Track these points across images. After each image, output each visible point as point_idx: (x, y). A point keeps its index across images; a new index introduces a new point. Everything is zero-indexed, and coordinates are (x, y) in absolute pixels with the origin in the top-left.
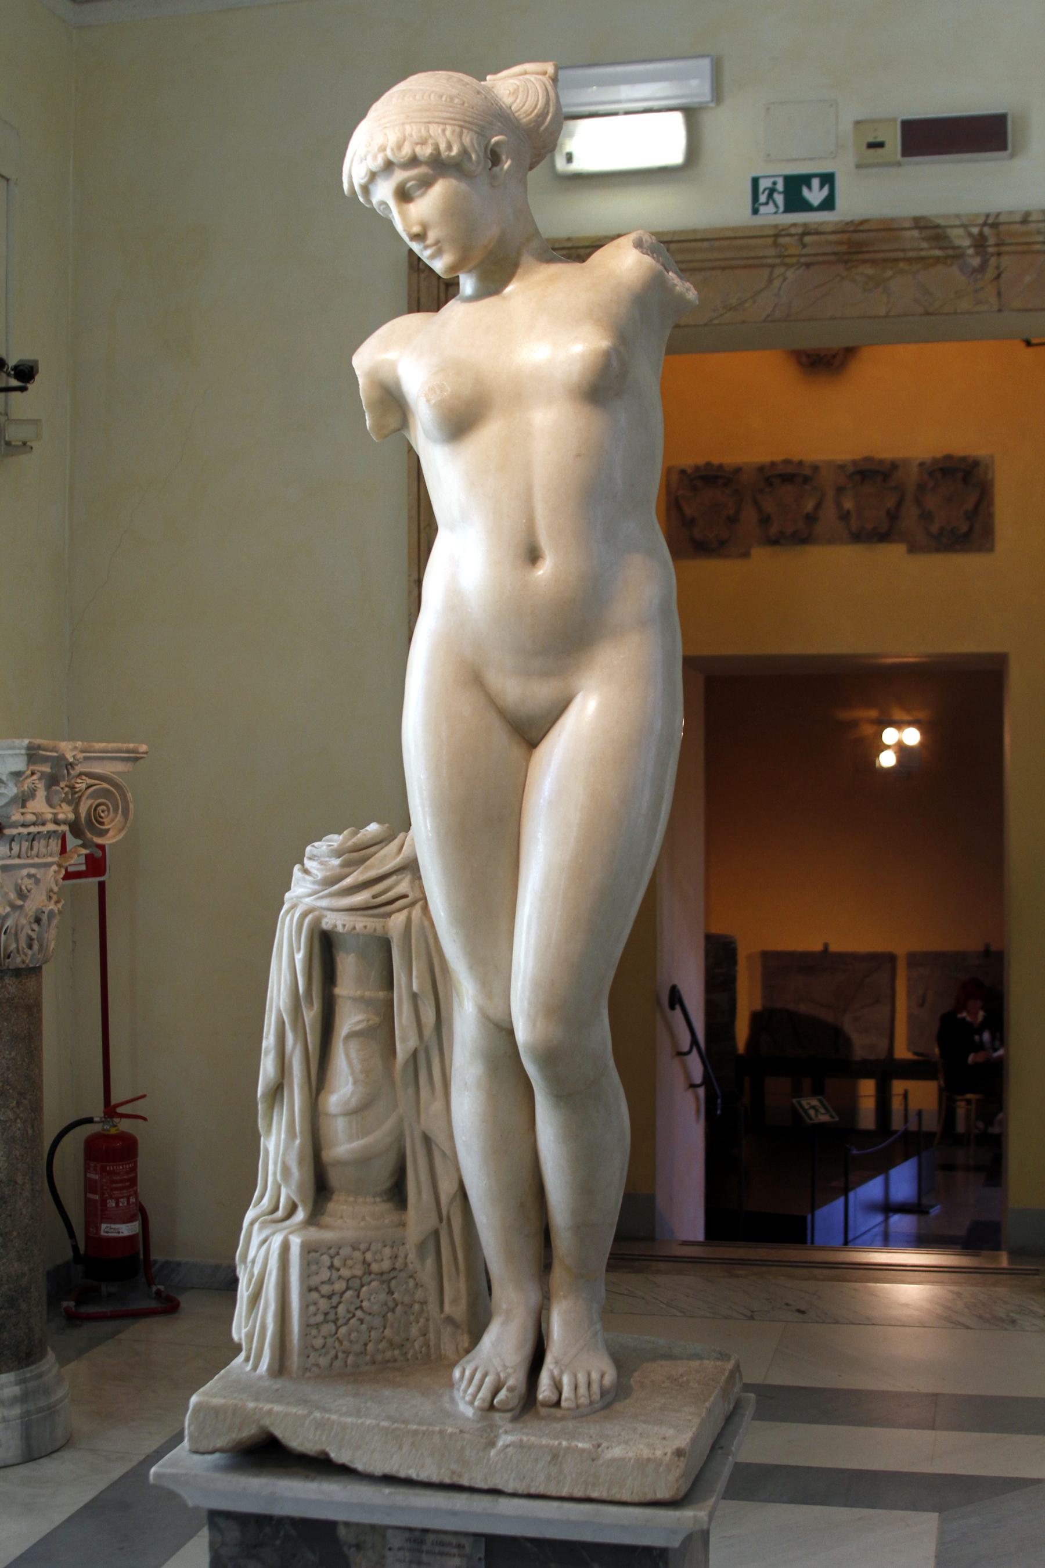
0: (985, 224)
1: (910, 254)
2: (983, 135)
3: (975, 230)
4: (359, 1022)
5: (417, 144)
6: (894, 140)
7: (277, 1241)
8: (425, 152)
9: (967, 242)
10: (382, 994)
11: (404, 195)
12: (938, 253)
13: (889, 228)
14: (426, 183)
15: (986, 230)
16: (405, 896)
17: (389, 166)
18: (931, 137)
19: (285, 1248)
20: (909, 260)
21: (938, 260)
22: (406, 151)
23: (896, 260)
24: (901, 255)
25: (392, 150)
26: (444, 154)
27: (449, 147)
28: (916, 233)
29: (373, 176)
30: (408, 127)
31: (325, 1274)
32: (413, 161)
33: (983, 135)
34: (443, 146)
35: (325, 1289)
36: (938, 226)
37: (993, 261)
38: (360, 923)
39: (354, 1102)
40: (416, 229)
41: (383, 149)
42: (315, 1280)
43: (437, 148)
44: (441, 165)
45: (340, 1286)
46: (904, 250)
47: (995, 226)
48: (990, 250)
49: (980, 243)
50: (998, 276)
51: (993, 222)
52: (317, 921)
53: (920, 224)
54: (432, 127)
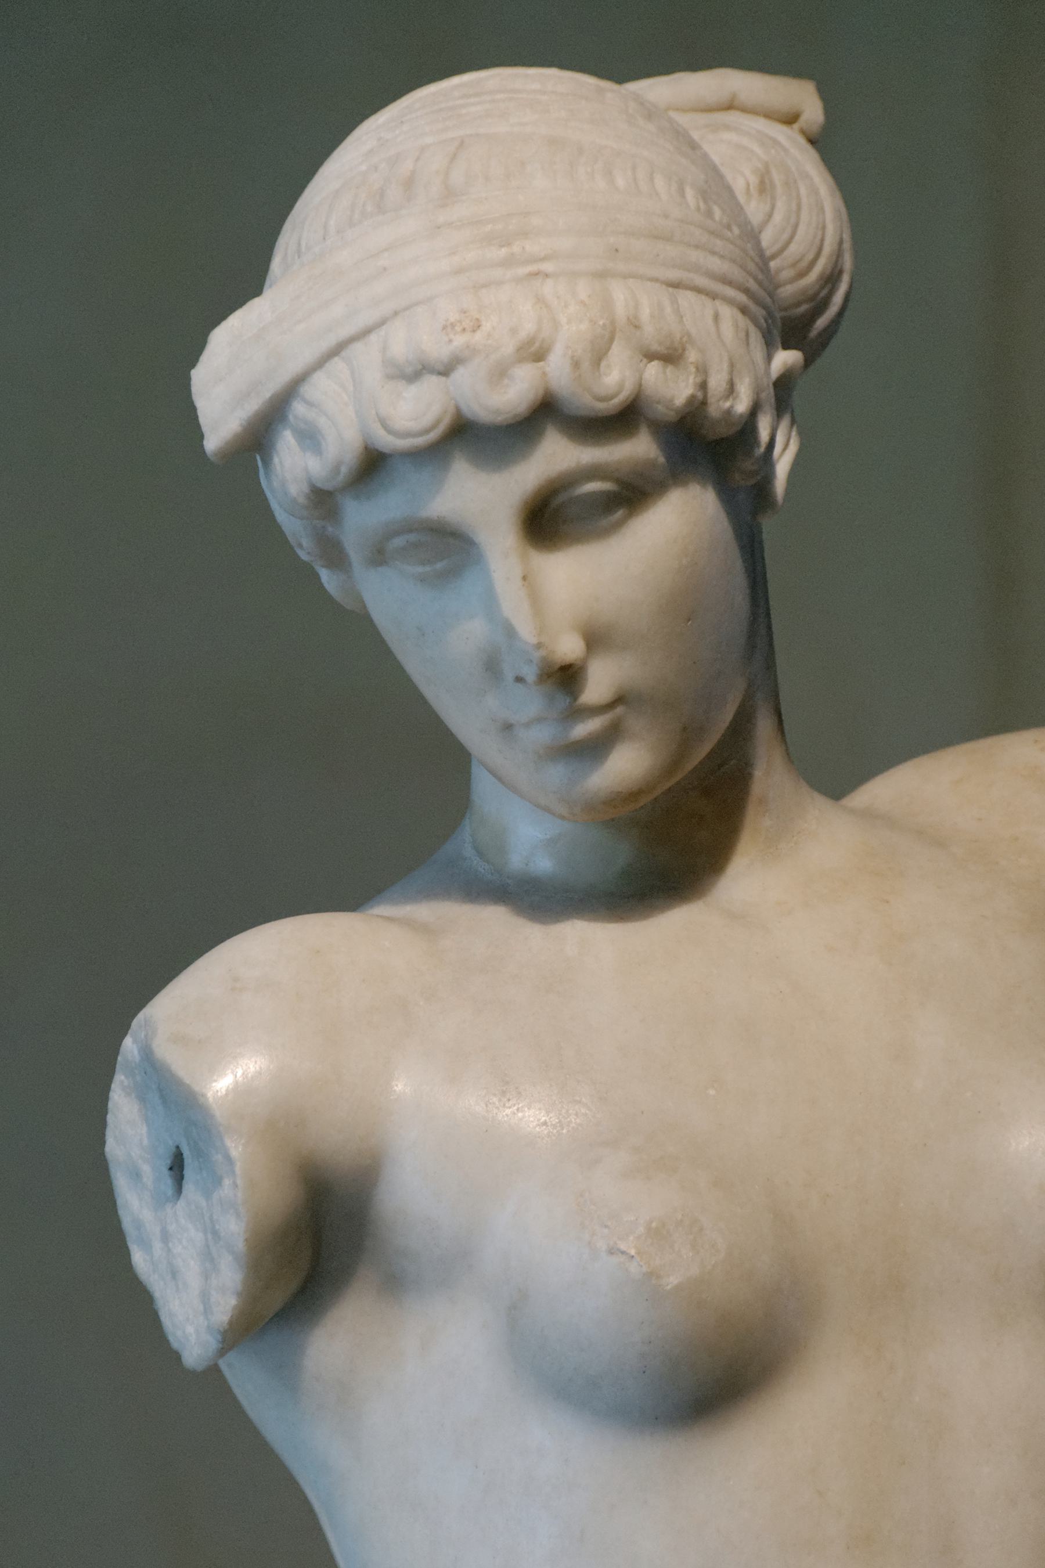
5: (651, 356)
8: (673, 389)
11: (547, 520)
14: (631, 494)
17: (546, 412)
22: (616, 378)
25: (576, 364)
26: (716, 408)
27: (731, 390)
29: (466, 436)
30: (620, 294)
32: (626, 418)
34: (717, 382)
40: (569, 647)
41: (535, 352)
43: (703, 386)
44: (706, 447)
54: (687, 299)
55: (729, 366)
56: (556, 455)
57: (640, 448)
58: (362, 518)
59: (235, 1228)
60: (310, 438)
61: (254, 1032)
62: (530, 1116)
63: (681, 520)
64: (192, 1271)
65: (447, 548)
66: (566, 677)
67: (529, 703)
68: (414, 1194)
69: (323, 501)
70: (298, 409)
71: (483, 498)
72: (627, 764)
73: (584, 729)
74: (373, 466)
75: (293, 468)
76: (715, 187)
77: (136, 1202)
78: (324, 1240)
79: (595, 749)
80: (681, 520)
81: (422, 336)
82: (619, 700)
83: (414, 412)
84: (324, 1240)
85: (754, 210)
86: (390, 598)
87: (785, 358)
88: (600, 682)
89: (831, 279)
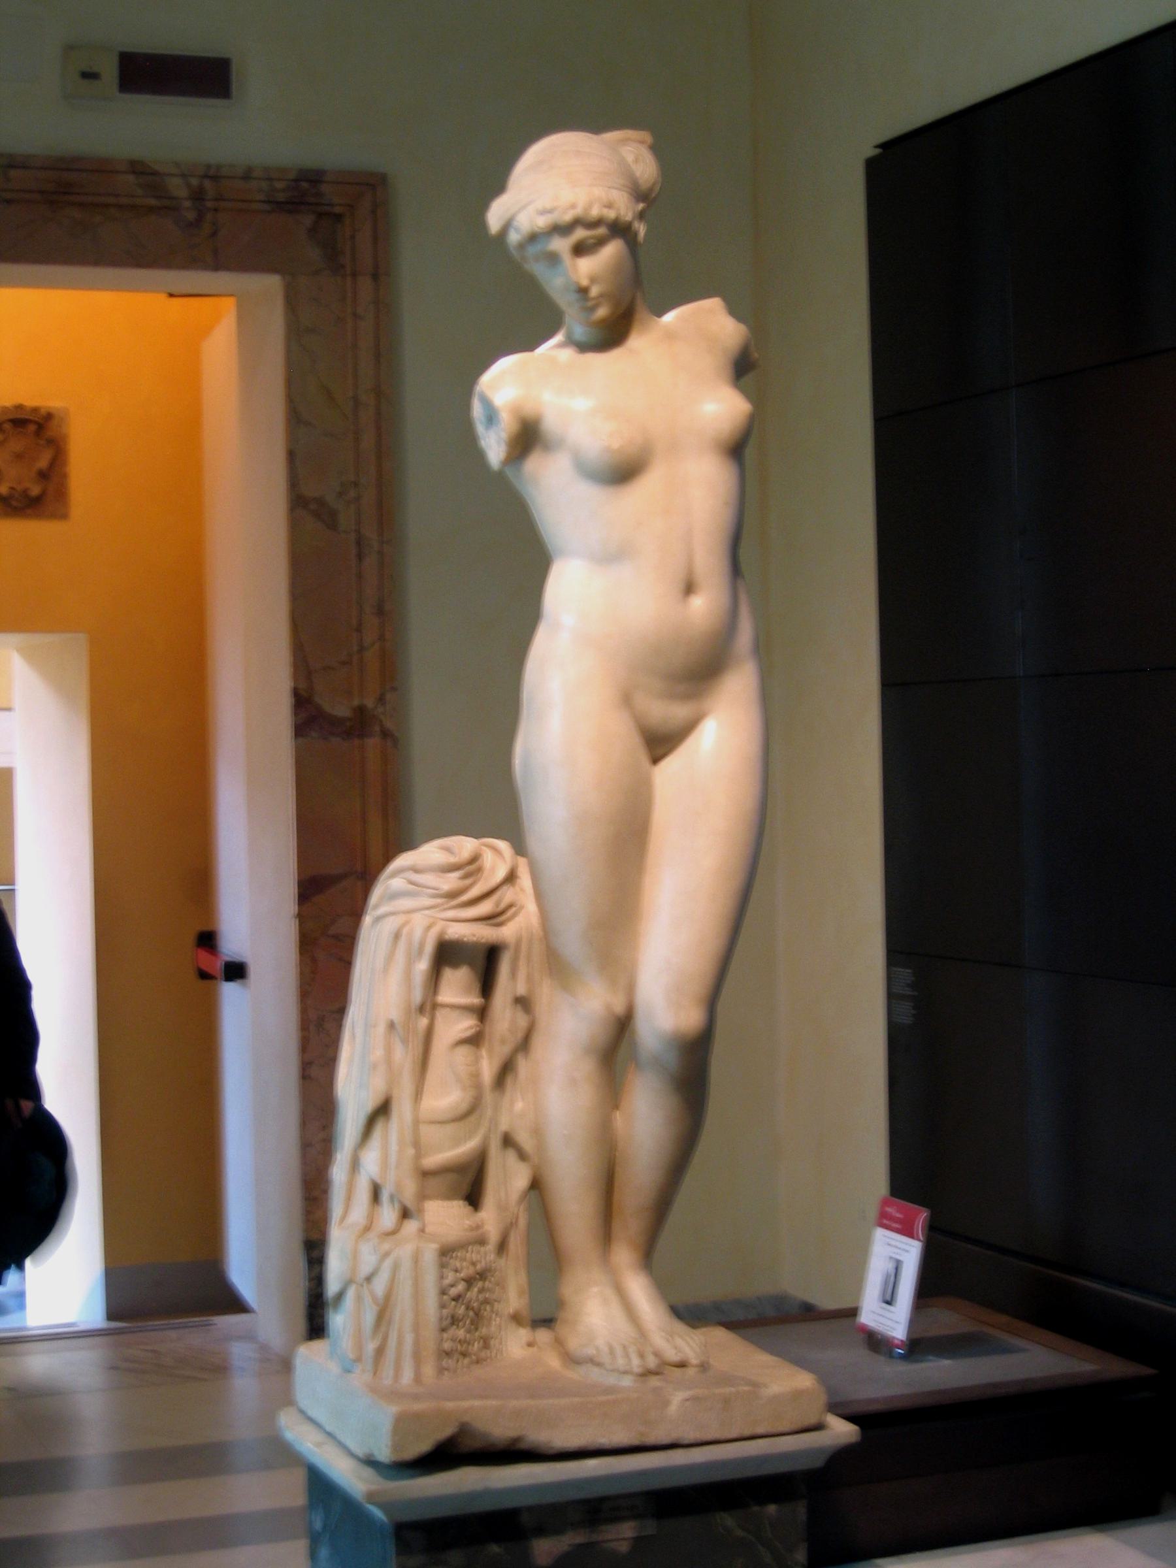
0: (206, 176)
1: (124, 201)
2: (206, 77)
3: (194, 182)
4: (466, 1029)
6: (110, 70)
7: (405, 1252)
8: (611, 214)
9: (183, 193)
10: (476, 1000)
11: (580, 250)
12: (153, 202)
13: (102, 168)
14: (601, 242)
15: (207, 184)
16: (510, 906)
17: (577, 223)
18: (146, 73)
19: (416, 1259)
20: (120, 207)
21: (151, 209)
22: (595, 212)
23: (107, 206)
24: (112, 200)
28: (131, 178)
31: (450, 1277)
33: (206, 77)
34: (622, 213)
35: (453, 1292)
36: (155, 173)
37: (209, 216)
38: (484, 934)
39: (464, 1107)
40: (584, 282)
41: (573, 206)
42: (447, 1282)
44: (619, 229)
45: (461, 1287)
46: (117, 196)
47: (215, 178)
48: (209, 204)
49: (198, 196)
50: (214, 234)
51: (213, 174)
52: (442, 933)
53: (137, 168)
55: (624, 208)
56: (580, 233)
57: (602, 231)
58: (532, 250)
59: (504, 435)
60: (517, 230)
61: (508, 384)
62: (581, 404)
63: (612, 250)
64: (494, 448)
65: (553, 259)
66: (583, 291)
67: (573, 297)
68: (551, 423)
69: (522, 246)
70: (515, 223)
71: (561, 245)
72: (602, 312)
73: (590, 304)
74: (533, 237)
75: (514, 237)
76: (622, 162)
77: (480, 429)
78: (528, 437)
79: (592, 309)
80: (612, 250)
81: (540, 204)
82: (601, 296)
83: (542, 222)
84: (528, 437)
85: (634, 167)
86: (538, 269)
87: (641, 206)
88: (595, 291)
89: (654, 184)
